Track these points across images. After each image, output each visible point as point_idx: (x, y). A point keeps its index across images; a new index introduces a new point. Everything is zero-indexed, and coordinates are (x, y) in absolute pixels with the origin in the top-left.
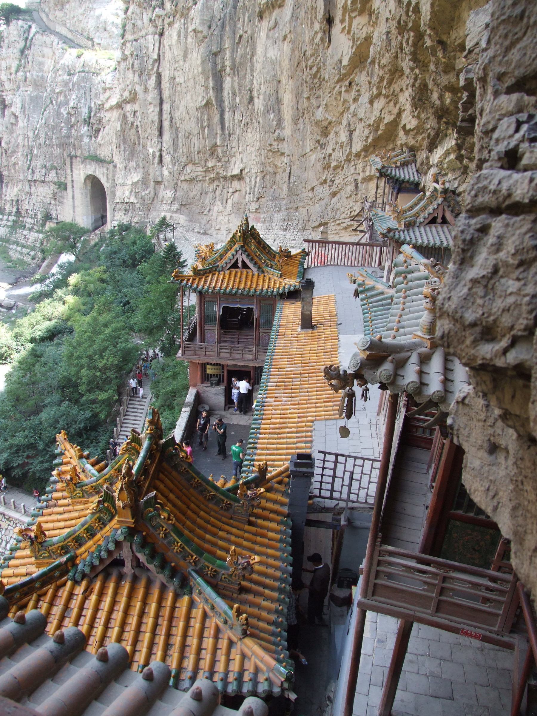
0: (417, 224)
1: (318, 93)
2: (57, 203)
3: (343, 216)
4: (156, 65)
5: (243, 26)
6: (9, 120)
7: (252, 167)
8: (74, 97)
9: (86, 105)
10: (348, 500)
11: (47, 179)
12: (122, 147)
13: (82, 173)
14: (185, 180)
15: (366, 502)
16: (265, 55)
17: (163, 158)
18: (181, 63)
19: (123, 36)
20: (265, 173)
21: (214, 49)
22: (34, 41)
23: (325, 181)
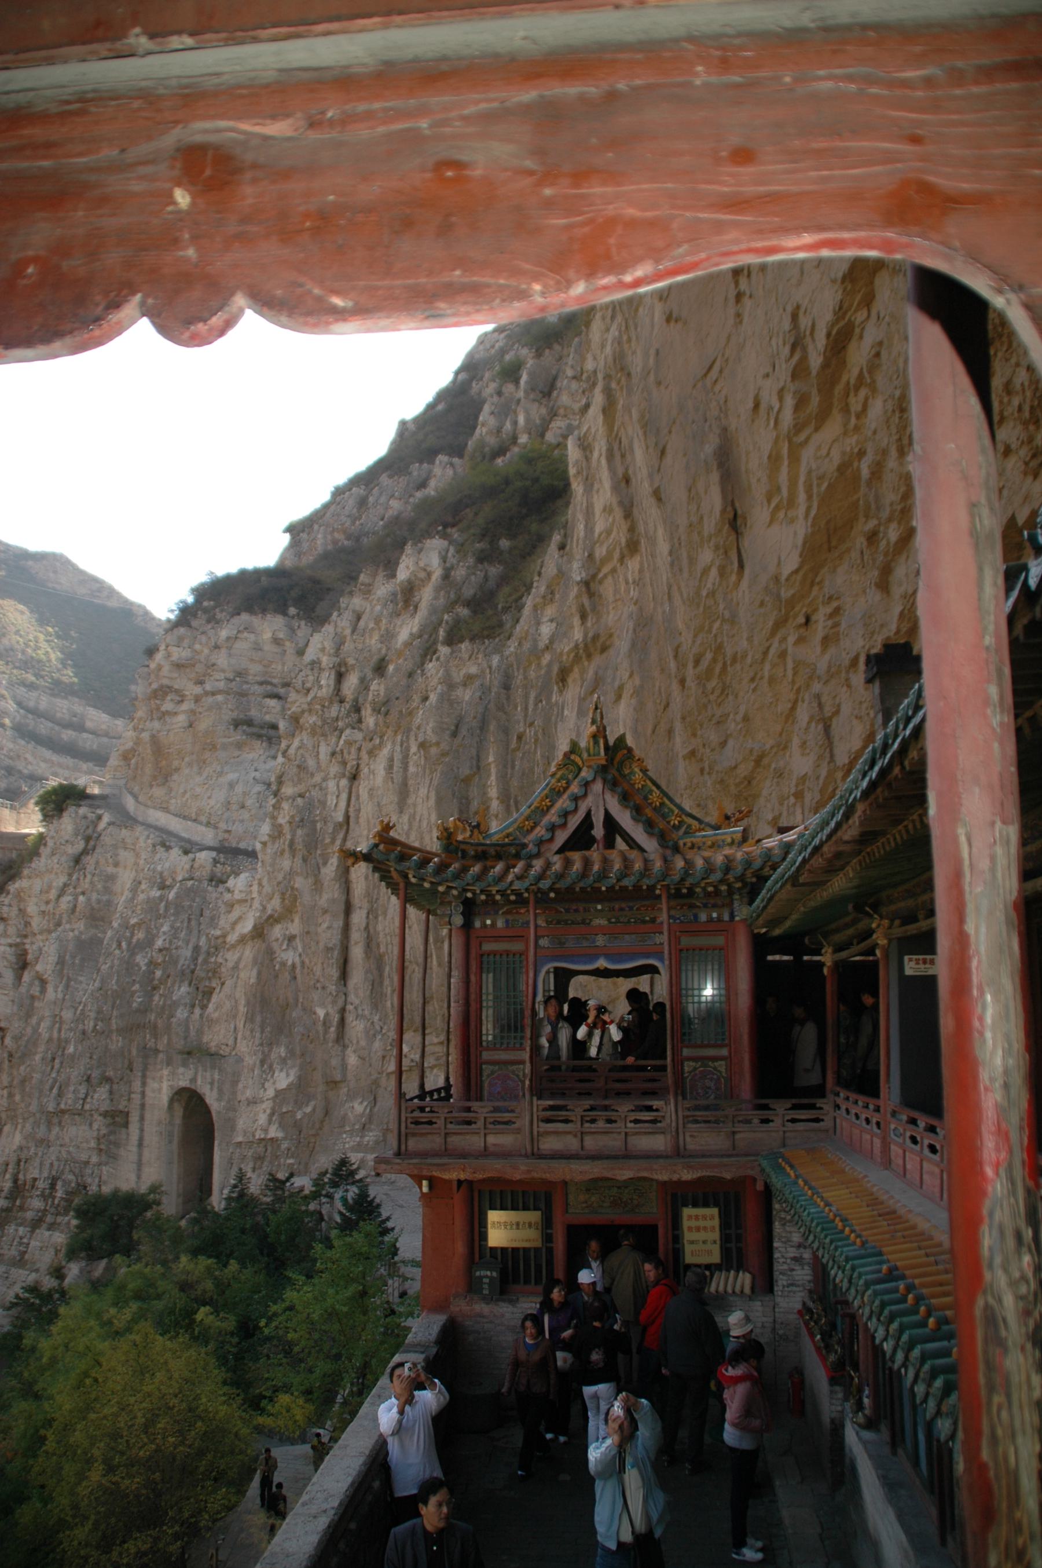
2: (104, 1158)
4: (341, 835)
5: (526, 716)
6: (28, 991)
8: (165, 928)
9: (187, 943)
11: (87, 1107)
12: (258, 1019)
13: (165, 1085)
17: (347, 1028)
21: (465, 771)
22: (102, 838)
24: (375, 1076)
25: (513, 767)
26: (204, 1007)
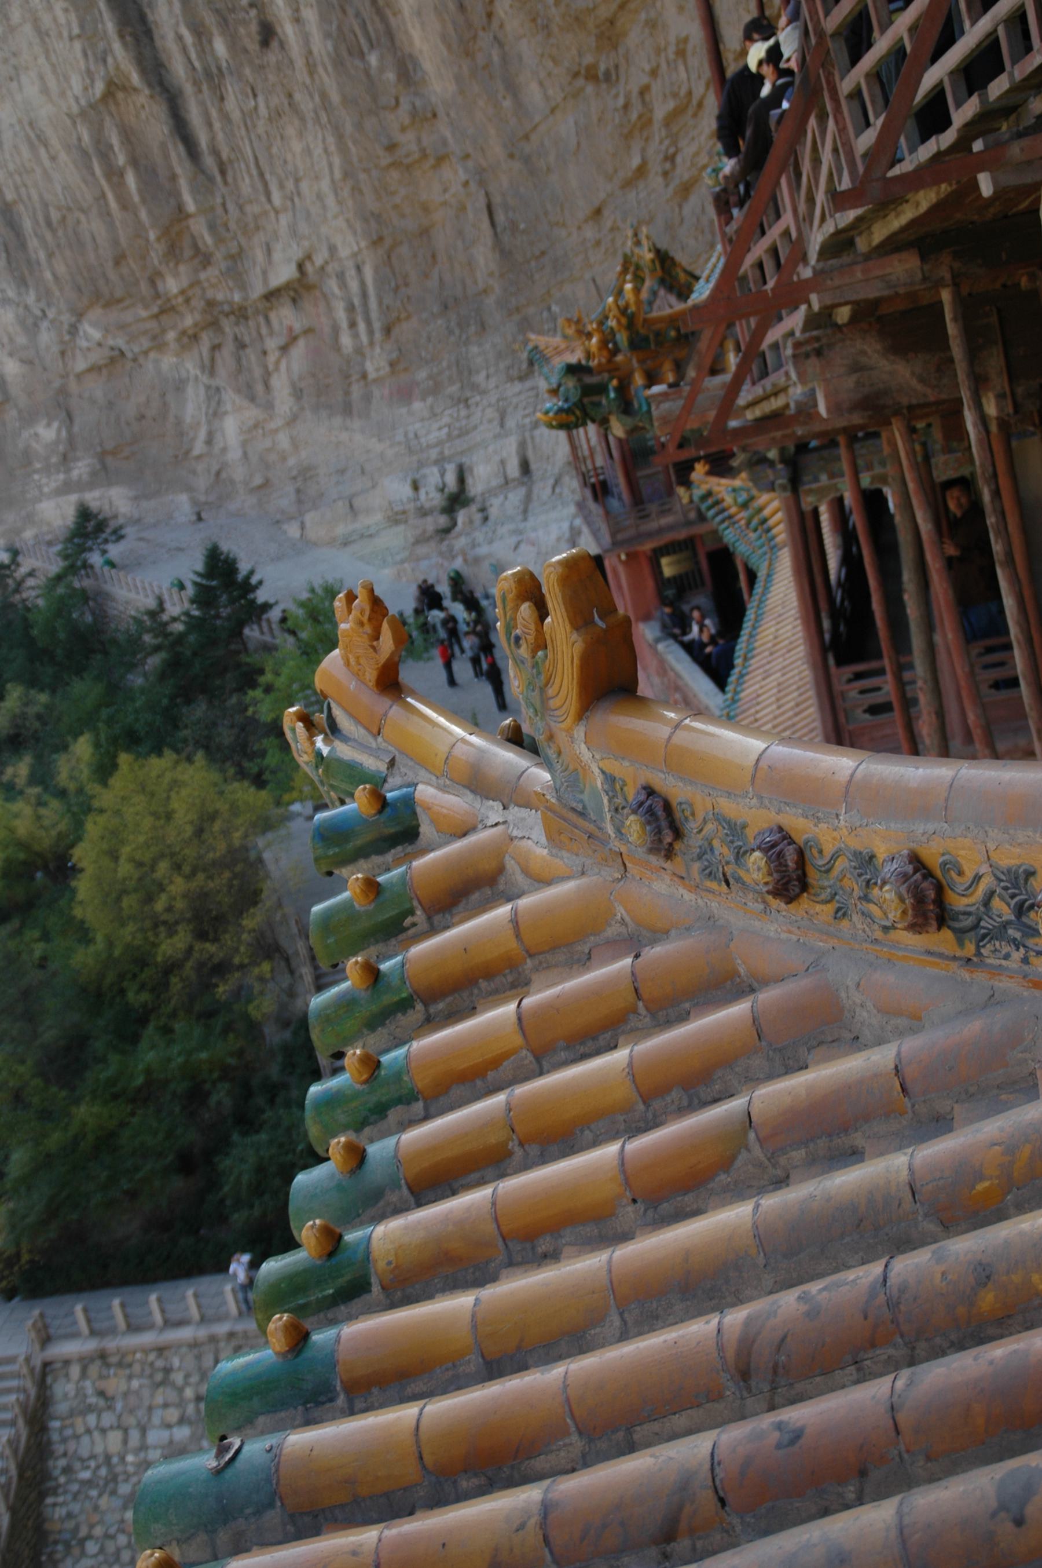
7: (338, 240)
20: (388, 242)
23: (641, 171)
24: (57, 384)
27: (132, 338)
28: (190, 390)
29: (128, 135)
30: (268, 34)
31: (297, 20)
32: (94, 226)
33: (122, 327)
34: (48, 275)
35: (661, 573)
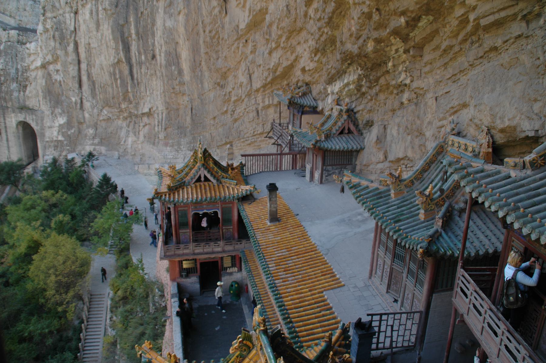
0: (332, 135)
1: (217, 49)
3: (248, 135)
4: (73, 35)
5: (144, 5)
10: (391, 347)
12: (48, 98)
13: (14, 120)
14: (104, 120)
15: (403, 346)
16: (164, 25)
18: (95, 33)
19: (44, 15)
23: (226, 112)
24: (96, 121)
25: (140, 23)
26: (24, 92)
27: (113, 115)
28: (123, 130)
29: (120, 72)
30: (154, 57)
31: (160, 55)
32: (110, 89)
33: (111, 112)
34: (98, 98)
35: (182, 266)
